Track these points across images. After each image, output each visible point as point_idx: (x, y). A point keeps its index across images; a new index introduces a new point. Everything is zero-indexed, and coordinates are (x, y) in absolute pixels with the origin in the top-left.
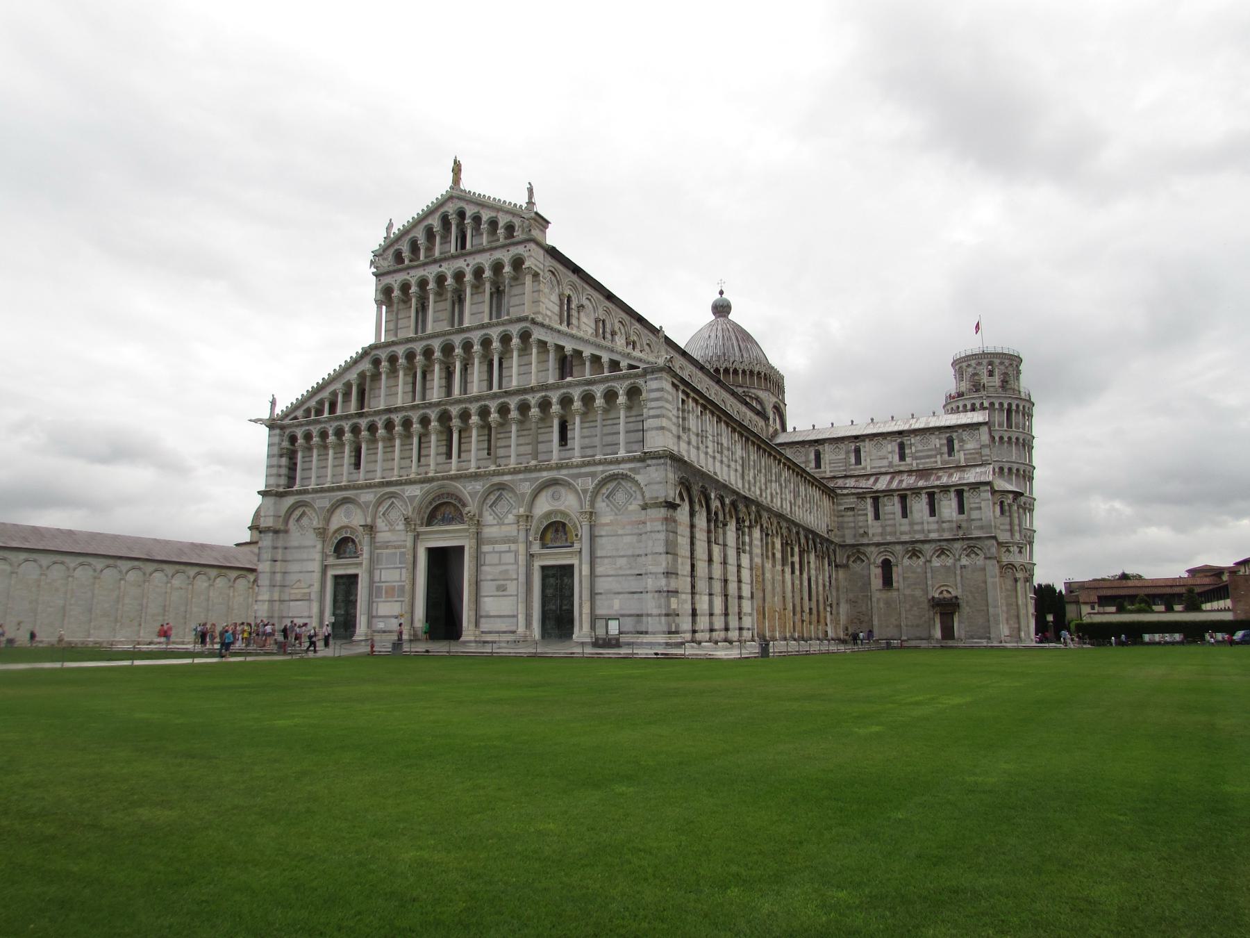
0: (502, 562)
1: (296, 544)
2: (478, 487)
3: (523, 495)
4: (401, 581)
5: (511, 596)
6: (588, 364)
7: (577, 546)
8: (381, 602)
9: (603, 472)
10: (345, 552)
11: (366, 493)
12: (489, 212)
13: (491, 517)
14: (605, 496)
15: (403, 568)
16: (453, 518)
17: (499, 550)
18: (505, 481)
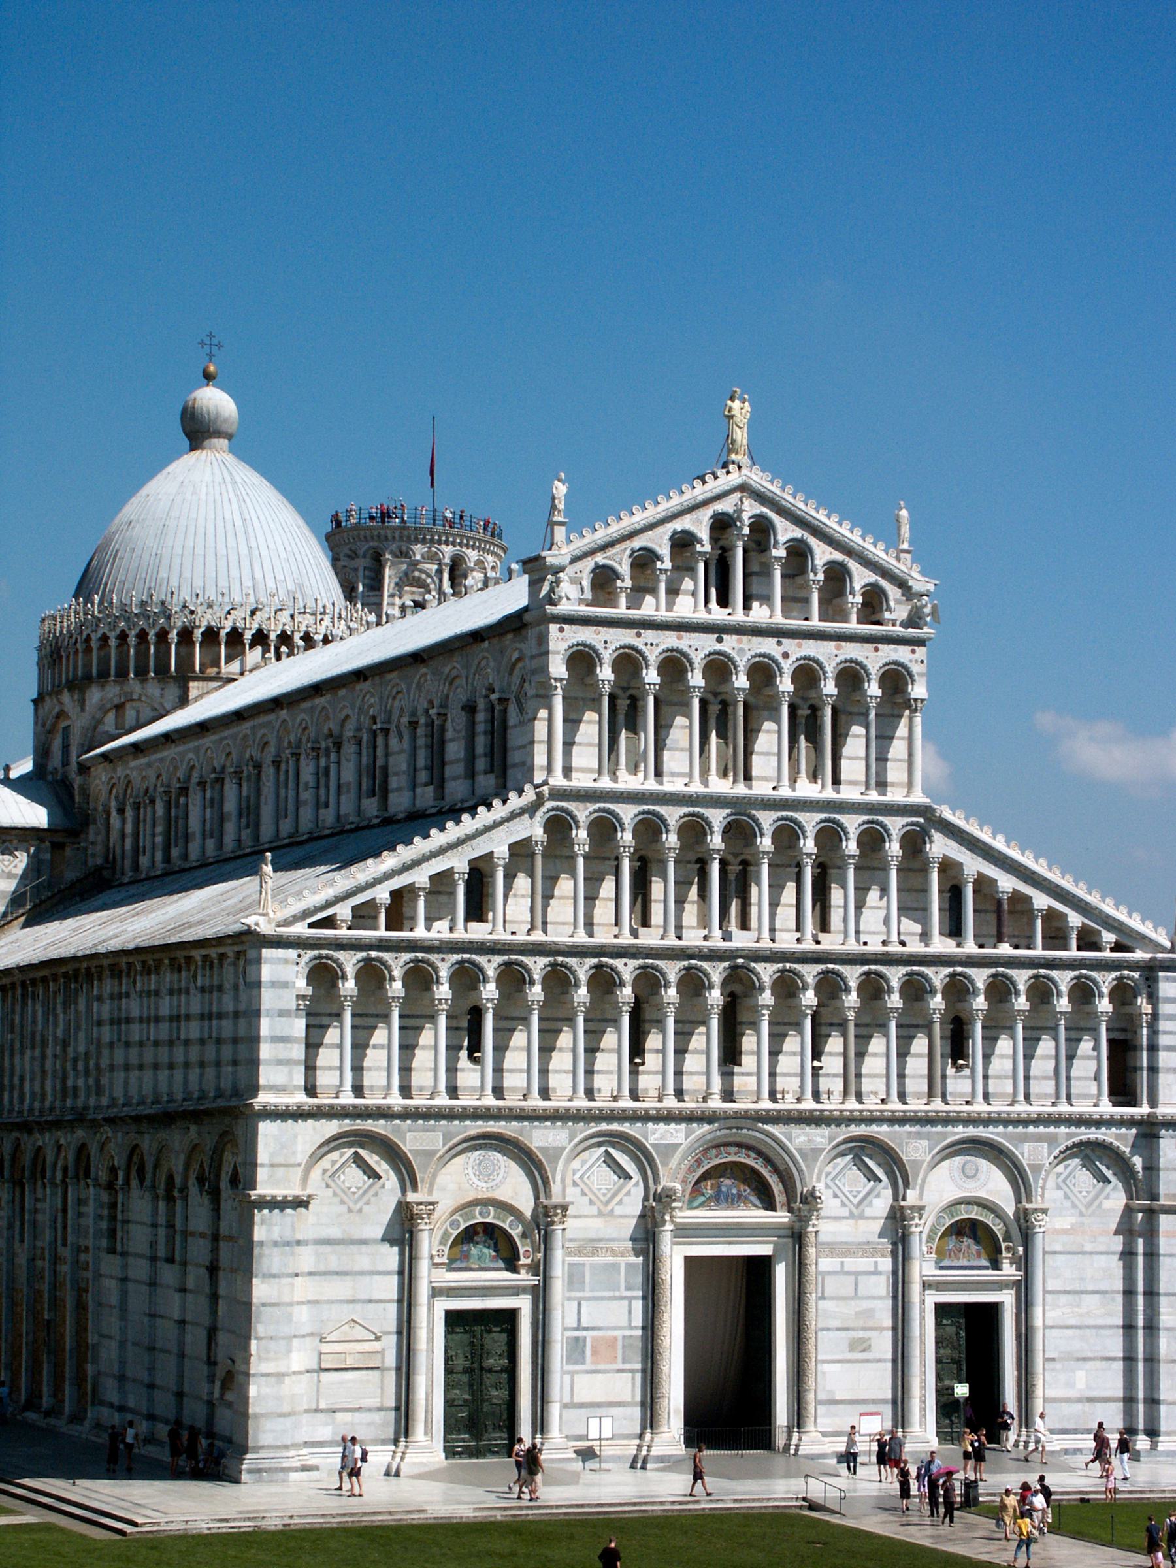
0: (860, 1294)
1: (335, 1232)
2: (818, 1139)
3: (917, 1164)
4: (631, 1328)
5: (879, 1361)
6: (1039, 922)
7: (1009, 1270)
8: (578, 1372)
9: (1069, 1136)
10: (466, 1256)
11: (546, 1127)
12: (830, 549)
13: (837, 1202)
14: (1063, 1177)
15: (635, 1298)
16: (739, 1196)
17: (853, 1269)
18: (878, 1133)
